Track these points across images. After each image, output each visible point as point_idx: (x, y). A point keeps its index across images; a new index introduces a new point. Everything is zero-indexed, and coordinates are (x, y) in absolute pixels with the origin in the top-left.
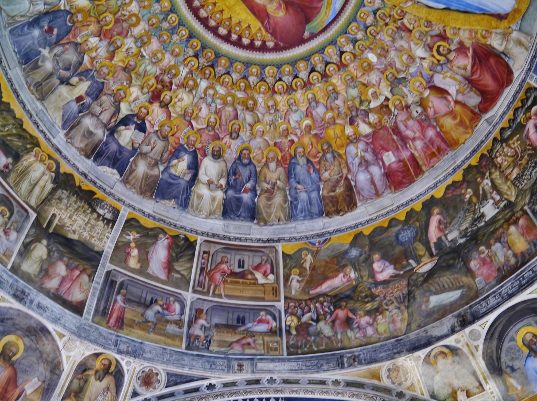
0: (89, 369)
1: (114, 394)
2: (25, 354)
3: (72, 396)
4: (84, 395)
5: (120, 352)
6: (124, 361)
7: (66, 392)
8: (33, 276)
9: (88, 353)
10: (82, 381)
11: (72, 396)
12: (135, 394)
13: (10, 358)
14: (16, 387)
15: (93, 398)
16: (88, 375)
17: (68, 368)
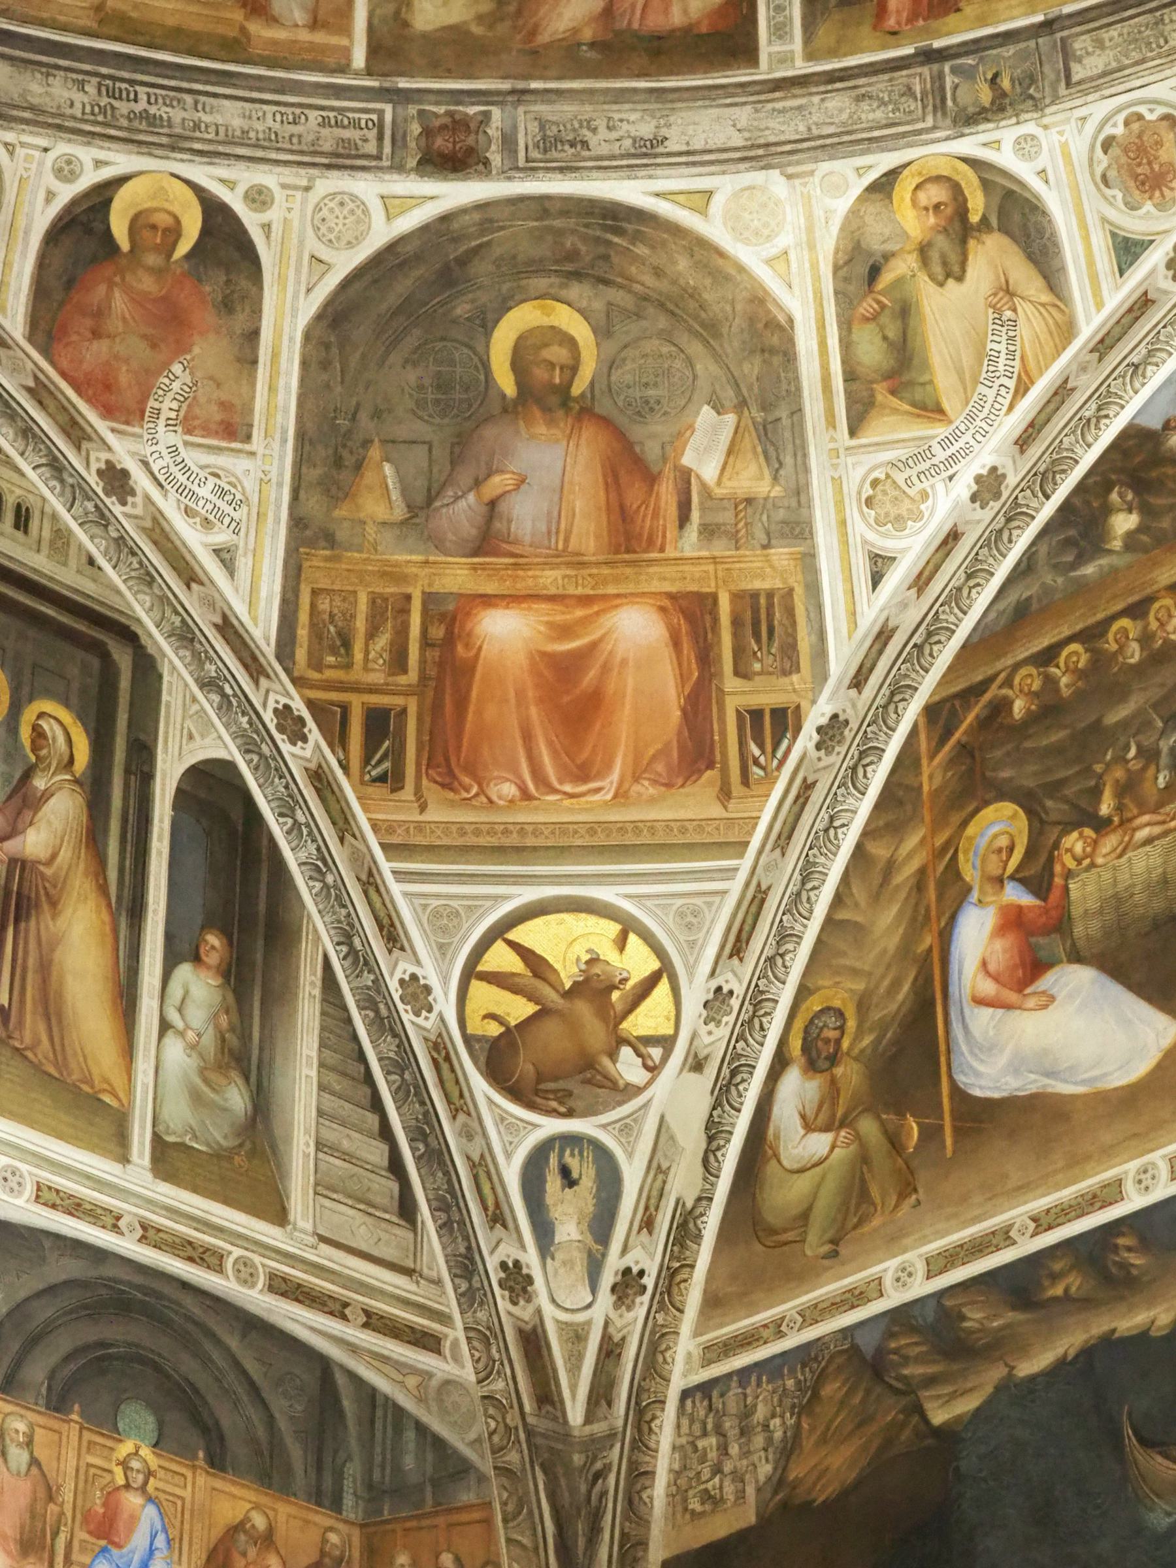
0: (887, 257)
1: (1046, 297)
2: (611, 347)
3: (881, 393)
4: (926, 366)
5: (969, 119)
6: (1003, 145)
7: (849, 394)
8: (477, 30)
9: (843, 204)
10: (885, 319)
11: (881, 393)
12: (1128, 250)
13: (564, 391)
14: (651, 479)
15: (967, 360)
16: (899, 282)
17: (805, 301)
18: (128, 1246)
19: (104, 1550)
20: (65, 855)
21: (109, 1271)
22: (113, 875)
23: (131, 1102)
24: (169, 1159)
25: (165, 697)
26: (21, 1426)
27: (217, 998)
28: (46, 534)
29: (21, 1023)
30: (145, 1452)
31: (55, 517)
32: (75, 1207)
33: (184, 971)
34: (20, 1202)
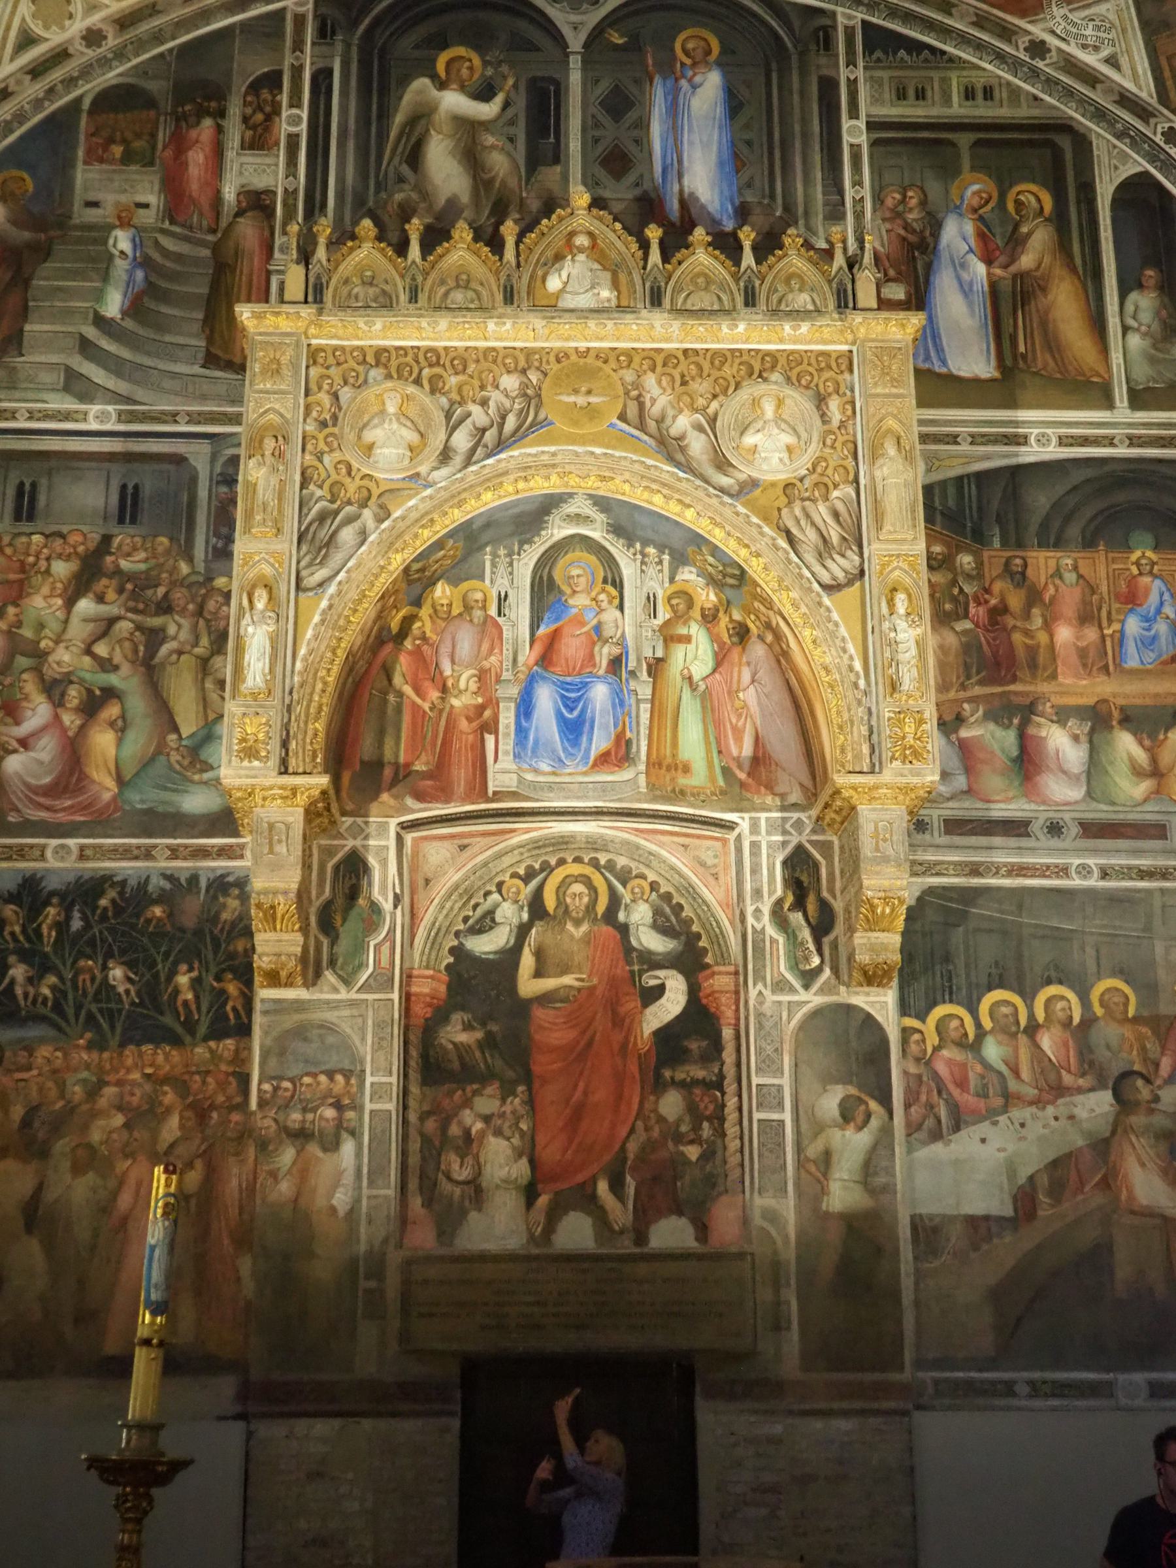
18: (1122, 451)
19: (1131, 610)
20: (1047, 260)
21: (1107, 468)
22: (1078, 261)
23: (1111, 376)
24: (1138, 399)
25: (1096, 153)
26: (1069, 562)
27: (1157, 303)
28: (1005, 95)
29: (1035, 359)
30: (1149, 554)
31: (1009, 84)
32: (1085, 441)
33: (1133, 296)
34: (1051, 449)
